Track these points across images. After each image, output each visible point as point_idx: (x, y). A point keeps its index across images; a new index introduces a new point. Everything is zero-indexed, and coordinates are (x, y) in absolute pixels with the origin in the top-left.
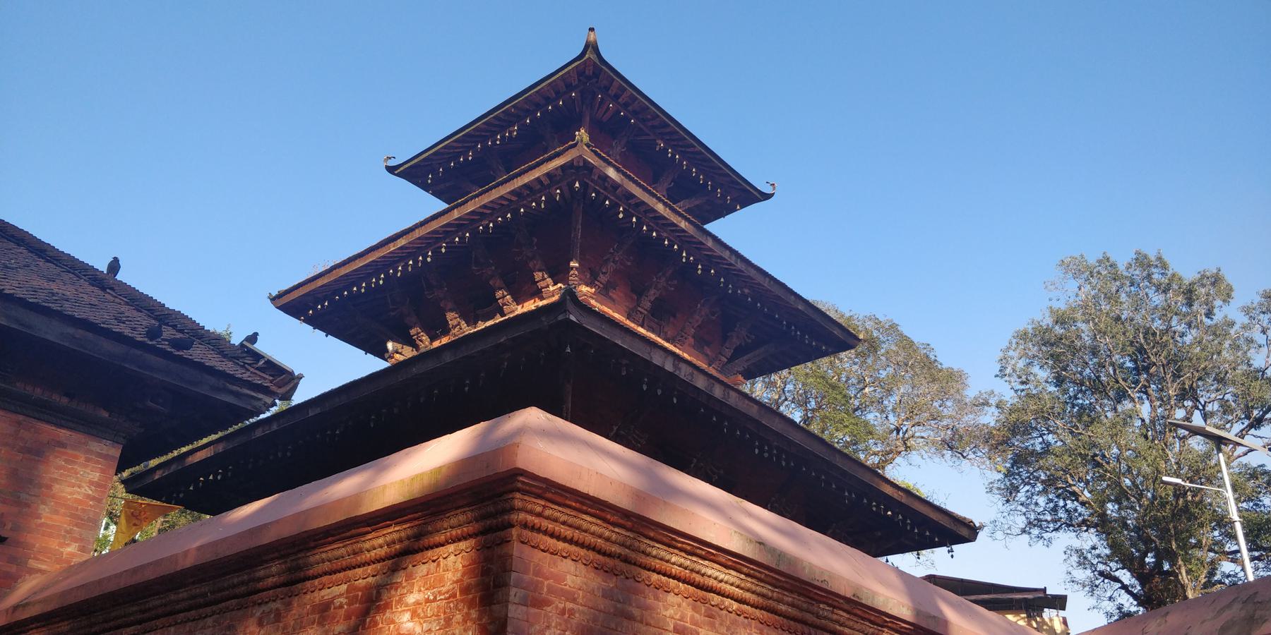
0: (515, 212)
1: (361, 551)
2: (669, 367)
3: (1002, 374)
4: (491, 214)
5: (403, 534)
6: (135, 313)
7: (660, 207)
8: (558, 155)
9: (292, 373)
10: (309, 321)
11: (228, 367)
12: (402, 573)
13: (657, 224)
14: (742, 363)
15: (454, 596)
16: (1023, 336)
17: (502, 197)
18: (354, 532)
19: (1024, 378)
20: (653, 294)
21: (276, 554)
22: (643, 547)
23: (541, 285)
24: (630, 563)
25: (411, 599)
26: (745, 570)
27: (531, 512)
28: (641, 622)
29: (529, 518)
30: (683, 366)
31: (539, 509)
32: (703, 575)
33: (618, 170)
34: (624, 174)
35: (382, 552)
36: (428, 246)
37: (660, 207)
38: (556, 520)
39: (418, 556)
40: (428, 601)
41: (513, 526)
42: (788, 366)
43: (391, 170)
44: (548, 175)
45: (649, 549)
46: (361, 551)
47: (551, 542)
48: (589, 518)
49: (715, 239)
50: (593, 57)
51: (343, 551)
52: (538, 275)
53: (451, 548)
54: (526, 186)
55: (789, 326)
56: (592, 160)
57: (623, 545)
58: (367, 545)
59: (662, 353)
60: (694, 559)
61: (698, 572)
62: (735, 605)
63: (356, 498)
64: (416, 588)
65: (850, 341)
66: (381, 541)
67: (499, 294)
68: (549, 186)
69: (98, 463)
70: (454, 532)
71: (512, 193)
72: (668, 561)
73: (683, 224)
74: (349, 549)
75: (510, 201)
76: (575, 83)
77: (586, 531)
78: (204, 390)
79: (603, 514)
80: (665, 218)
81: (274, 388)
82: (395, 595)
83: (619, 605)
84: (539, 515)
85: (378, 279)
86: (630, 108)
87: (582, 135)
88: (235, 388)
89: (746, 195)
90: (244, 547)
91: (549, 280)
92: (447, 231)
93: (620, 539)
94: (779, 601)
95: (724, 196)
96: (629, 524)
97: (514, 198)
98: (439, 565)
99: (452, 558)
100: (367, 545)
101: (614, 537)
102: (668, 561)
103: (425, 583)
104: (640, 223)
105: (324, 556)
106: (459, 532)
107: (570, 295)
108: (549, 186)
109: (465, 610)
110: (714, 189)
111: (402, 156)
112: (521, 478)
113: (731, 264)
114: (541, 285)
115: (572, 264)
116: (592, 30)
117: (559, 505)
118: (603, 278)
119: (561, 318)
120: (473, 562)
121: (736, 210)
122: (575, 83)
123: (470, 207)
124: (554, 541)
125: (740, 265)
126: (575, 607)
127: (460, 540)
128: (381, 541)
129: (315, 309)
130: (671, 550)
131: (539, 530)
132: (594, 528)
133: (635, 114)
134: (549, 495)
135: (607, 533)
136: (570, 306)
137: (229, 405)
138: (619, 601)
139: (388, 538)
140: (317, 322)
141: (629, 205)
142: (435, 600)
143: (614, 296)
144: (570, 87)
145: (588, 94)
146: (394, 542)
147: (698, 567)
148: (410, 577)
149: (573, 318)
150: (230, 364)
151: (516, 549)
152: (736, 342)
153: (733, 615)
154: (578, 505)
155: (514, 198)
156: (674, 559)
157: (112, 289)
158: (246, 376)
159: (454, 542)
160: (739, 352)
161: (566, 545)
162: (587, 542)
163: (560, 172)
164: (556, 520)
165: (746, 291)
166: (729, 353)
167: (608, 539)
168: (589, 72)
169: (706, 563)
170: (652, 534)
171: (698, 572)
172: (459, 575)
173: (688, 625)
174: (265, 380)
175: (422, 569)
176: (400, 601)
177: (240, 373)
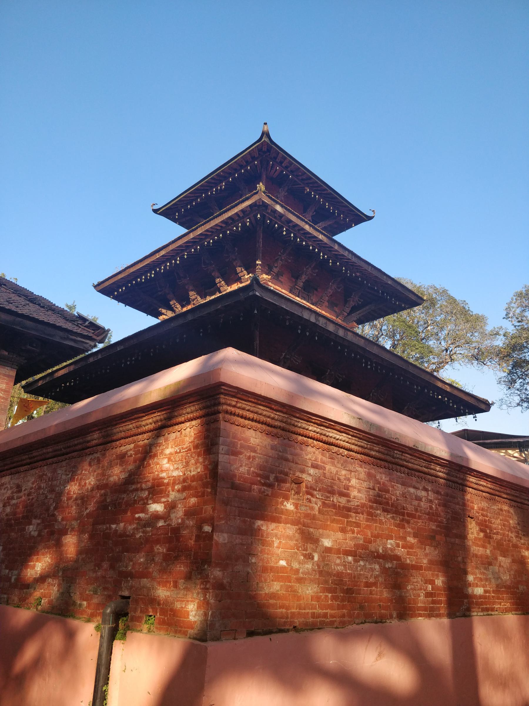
0: (224, 233)
1: (140, 426)
2: (313, 319)
3: (507, 317)
4: (211, 235)
5: (162, 417)
6: (18, 298)
7: (307, 227)
8: (247, 199)
9: (103, 329)
10: (116, 298)
11: (69, 326)
12: (162, 438)
13: (306, 237)
14: (356, 315)
15: (190, 450)
16: (520, 295)
17: (216, 225)
18: (136, 416)
19: (520, 319)
20: (304, 278)
21: (96, 428)
22: (293, 422)
23: (240, 275)
24: (286, 431)
25: (168, 451)
26: (351, 433)
27: (230, 405)
28: (293, 462)
29: (229, 408)
30: (321, 319)
31: (234, 403)
32: (327, 436)
33: (282, 206)
34: (286, 209)
35: (151, 427)
36: (177, 254)
37: (307, 227)
38: (244, 409)
39: (171, 429)
40: (176, 452)
41: (220, 413)
42: (383, 316)
43: (155, 211)
44: (242, 211)
45: (296, 423)
46: (140, 426)
47: (242, 420)
48: (262, 408)
49: (339, 244)
51: (131, 426)
52: (239, 269)
53: (188, 424)
54: (230, 218)
55: (383, 293)
56: (267, 201)
57: (281, 421)
58: (144, 423)
59: (309, 312)
60: (322, 428)
61: (324, 435)
62: (346, 452)
63: (137, 398)
64: (170, 446)
65: (419, 301)
66: (150, 421)
67: (217, 280)
68: (243, 217)
69: (4, 379)
70: (189, 416)
71: (222, 222)
72: (307, 429)
73: (321, 237)
74: (134, 425)
75: (221, 227)
76: (257, 155)
77: (260, 414)
78: (57, 339)
79: (270, 405)
80: (310, 234)
81: (95, 337)
82: (159, 449)
83: (280, 454)
84: (234, 406)
85: (151, 274)
86: (289, 169)
87: (261, 186)
88: (73, 337)
89: (357, 217)
90: (79, 425)
91: (245, 272)
92: (187, 246)
93: (280, 418)
94: (371, 449)
95: (344, 219)
96: (285, 410)
97: (224, 225)
98: (181, 433)
99: (188, 429)
100: (144, 423)
101: (276, 417)
102: (307, 429)
103: (175, 443)
104: (295, 237)
105: (121, 429)
106: (192, 416)
107: (255, 280)
108: (243, 217)
109: (196, 457)
110: (339, 215)
111: (162, 202)
112: (223, 387)
113: (349, 259)
114: (240, 275)
115: (257, 262)
116: (265, 124)
117: (246, 401)
118: (275, 270)
119: (251, 294)
120: (200, 432)
121: (351, 227)
122: (257, 155)
123: (199, 231)
124: (243, 420)
125: (354, 259)
126: (256, 455)
127: (192, 420)
128: (150, 421)
129: (118, 292)
130: (309, 423)
131: (234, 414)
132: (265, 413)
133: (292, 172)
134: (239, 396)
135: (273, 415)
136: (256, 287)
137: (71, 347)
138: (281, 452)
139: (154, 419)
140: (120, 298)
141: (289, 226)
142: (180, 452)
143: (282, 280)
144: (254, 159)
145: (265, 162)
146: (157, 421)
147: (324, 432)
148: (166, 440)
149: (257, 294)
150: (70, 324)
151: (223, 425)
152: (352, 304)
153: (345, 458)
154: (255, 401)
155: (224, 225)
156: (310, 428)
157: (5, 285)
158: (79, 331)
159: (189, 421)
160: (354, 309)
161: (250, 422)
162: (262, 420)
163: (249, 209)
164: (244, 409)
165: (358, 274)
166: (348, 310)
167: (273, 419)
168: (264, 149)
169: (329, 430)
170: (298, 415)
171: (324, 435)
172: (192, 438)
173: (319, 463)
174: (90, 333)
175: (173, 436)
176: (162, 453)
177: (76, 329)
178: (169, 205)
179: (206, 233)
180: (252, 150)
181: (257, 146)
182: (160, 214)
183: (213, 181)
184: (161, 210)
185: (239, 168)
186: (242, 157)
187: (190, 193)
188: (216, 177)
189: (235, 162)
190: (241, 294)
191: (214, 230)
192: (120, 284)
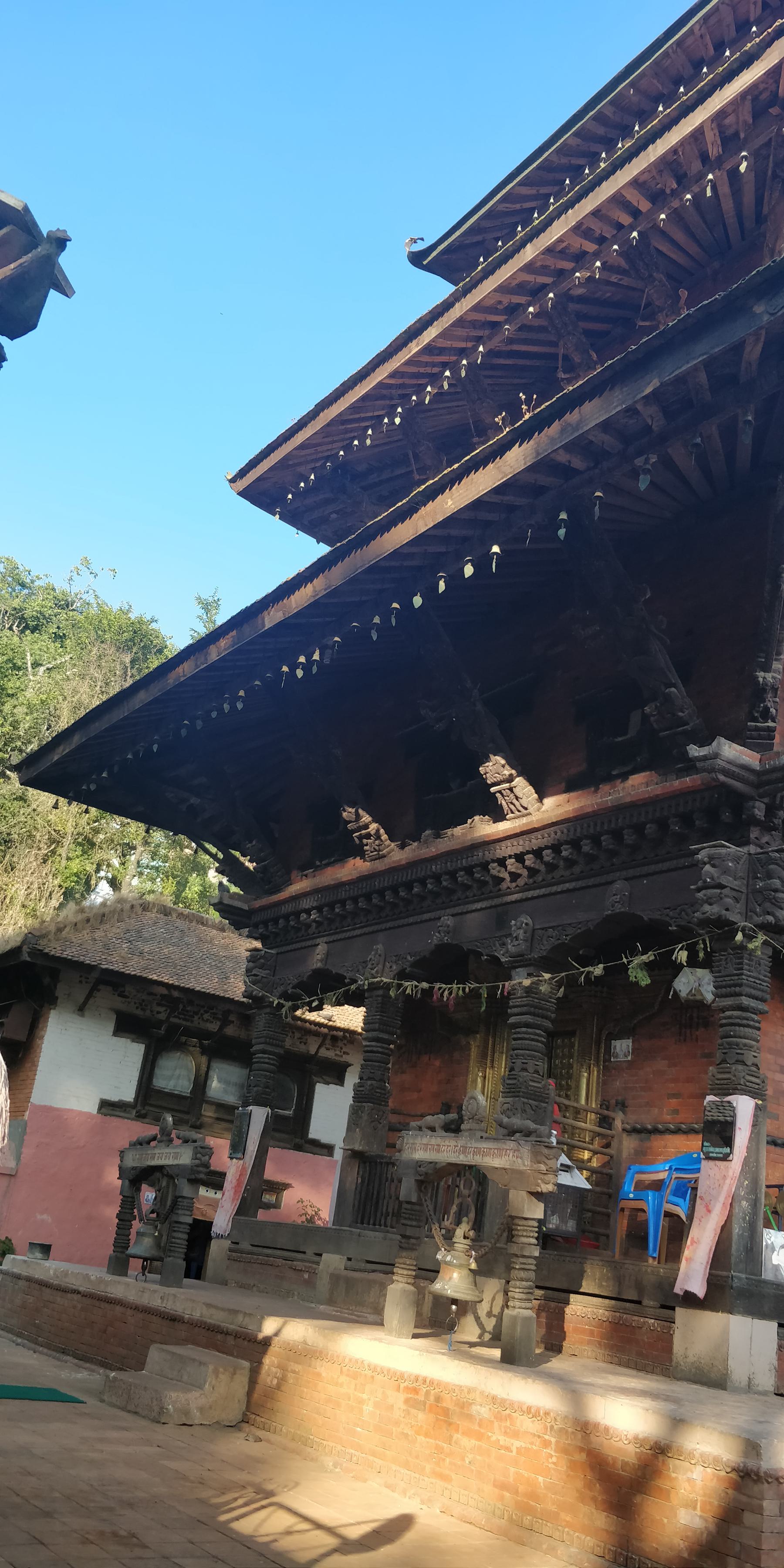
17: (617, 199)
44: (720, 116)
54: (669, 163)
75: (635, 213)
97: (644, 206)
155: (644, 206)
163: (746, 115)
178: (458, 233)
182: (428, 268)
183: (601, 131)
184: (434, 254)
185: (689, 71)
186: (706, 18)
188: (609, 112)
189: (679, 43)
190: (759, 309)
191: (608, 232)
192: (302, 469)
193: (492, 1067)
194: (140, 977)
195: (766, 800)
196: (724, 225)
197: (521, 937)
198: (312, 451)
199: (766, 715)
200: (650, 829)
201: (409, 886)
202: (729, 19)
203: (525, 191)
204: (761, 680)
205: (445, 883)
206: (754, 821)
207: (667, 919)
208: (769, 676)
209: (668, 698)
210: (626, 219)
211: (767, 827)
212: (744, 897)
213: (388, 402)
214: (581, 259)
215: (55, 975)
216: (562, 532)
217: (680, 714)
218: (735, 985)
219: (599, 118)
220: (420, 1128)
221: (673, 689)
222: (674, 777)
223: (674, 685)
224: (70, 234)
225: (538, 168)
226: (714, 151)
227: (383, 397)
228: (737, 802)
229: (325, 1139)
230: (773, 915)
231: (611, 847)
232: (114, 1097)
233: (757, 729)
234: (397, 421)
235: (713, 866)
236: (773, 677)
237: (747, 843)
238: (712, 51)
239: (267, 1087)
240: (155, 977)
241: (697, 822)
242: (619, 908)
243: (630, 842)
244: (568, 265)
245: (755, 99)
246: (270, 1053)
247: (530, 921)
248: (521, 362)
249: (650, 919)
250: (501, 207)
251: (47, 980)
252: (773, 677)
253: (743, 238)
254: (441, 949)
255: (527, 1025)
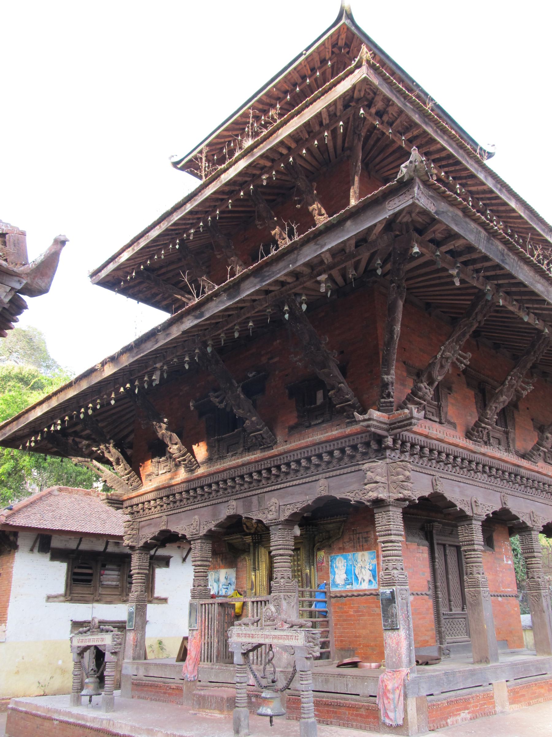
17: (282, 143)
50: (348, 22)
75: (289, 148)
97: (293, 145)
111: (182, 151)
155: (293, 145)
179: (263, 162)
180: (323, 44)
181: (331, 36)
183: (261, 106)
184: (183, 163)
185: (300, 81)
187: (225, 130)
188: (264, 99)
189: (295, 69)
193: (259, 570)
194: (61, 530)
195: (393, 437)
196: (328, 152)
197: (274, 510)
198: (132, 261)
199: (389, 395)
200: (337, 453)
201: (210, 486)
202: (317, 59)
203: (226, 133)
204: (386, 379)
205: (229, 484)
206: (388, 447)
207: (349, 498)
208: (389, 377)
209: (340, 389)
210: (284, 151)
211: (393, 450)
212: (387, 485)
213: (170, 237)
214: (263, 169)
215: (16, 534)
216: (287, 316)
217: (347, 397)
218: (388, 530)
219: (259, 101)
220: (240, 625)
221: (342, 385)
222: (345, 426)
223: (343, 383)
224: (68, 237)
225: (233, 123)
226: (326, 121)
227: (168, 235)
228: (380, 439)
229: (163, 596)
230: (402, 493)
231: (317, 463)
232: (54, 593)
233: (385, 402)
234: (177, 247)
235: (372, 472)
236: (392, 378)
237: (385, 458)
238: (310, 72)
239: (142, 591)
240: (69, 529)
241: (360, 449)
242: (324, 493)
243: (326, 460)
244: (258, 172)
245: (344, 98)
246: (141, 573)
247: (277, 502)
248: (233, 215)
249: (340, 498)
250: (215, 141)
251: (12, 538)
252: (392, 378)
253: (336, 158)
254: (229, 517)
255: (281, 555)
